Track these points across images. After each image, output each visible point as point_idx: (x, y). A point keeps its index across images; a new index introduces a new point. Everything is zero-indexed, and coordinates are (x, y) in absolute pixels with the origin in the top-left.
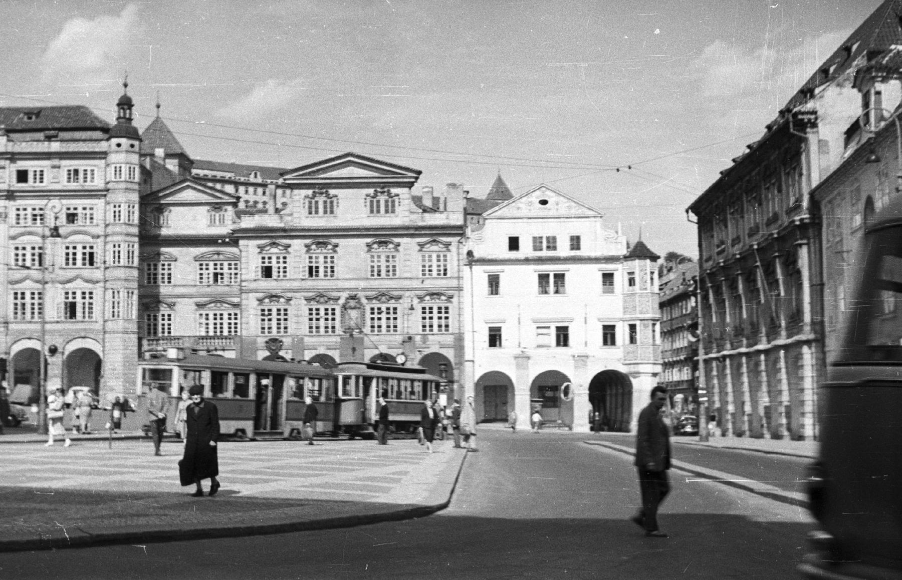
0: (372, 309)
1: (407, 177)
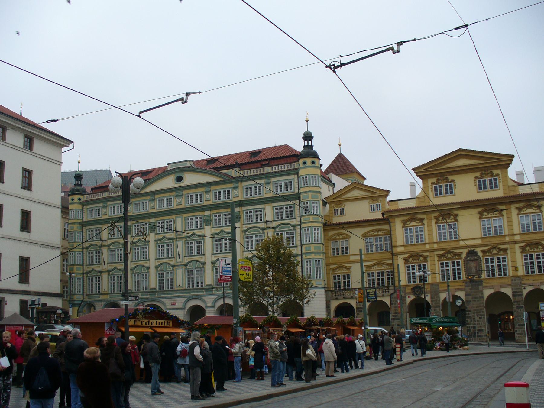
0: (487, 260)
1: (505, 161)
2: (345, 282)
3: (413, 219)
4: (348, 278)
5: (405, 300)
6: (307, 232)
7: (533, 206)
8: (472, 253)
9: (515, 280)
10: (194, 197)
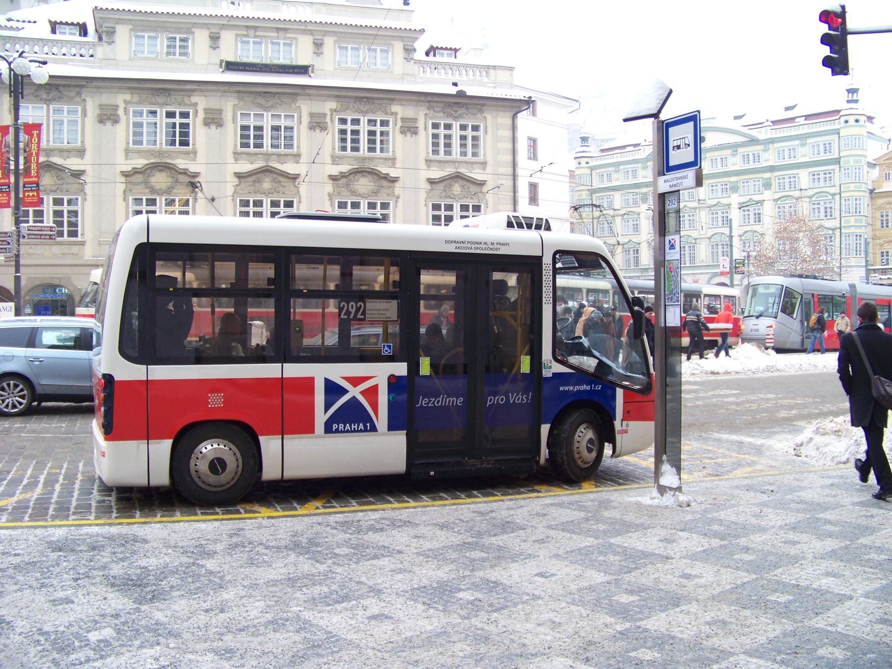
6: (847, 202)
10: (719, 161)
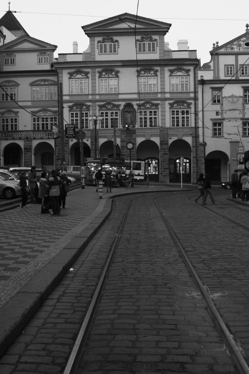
1: (163, 28)
2: (12, 125)
3: (79, 72)
4: (16, 122)
5: (68, 143)
7: (183, 70)
8: (129, 106)
9: (163, 131)
